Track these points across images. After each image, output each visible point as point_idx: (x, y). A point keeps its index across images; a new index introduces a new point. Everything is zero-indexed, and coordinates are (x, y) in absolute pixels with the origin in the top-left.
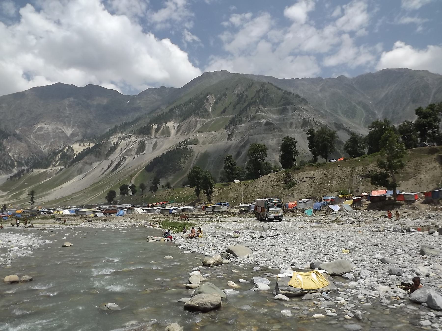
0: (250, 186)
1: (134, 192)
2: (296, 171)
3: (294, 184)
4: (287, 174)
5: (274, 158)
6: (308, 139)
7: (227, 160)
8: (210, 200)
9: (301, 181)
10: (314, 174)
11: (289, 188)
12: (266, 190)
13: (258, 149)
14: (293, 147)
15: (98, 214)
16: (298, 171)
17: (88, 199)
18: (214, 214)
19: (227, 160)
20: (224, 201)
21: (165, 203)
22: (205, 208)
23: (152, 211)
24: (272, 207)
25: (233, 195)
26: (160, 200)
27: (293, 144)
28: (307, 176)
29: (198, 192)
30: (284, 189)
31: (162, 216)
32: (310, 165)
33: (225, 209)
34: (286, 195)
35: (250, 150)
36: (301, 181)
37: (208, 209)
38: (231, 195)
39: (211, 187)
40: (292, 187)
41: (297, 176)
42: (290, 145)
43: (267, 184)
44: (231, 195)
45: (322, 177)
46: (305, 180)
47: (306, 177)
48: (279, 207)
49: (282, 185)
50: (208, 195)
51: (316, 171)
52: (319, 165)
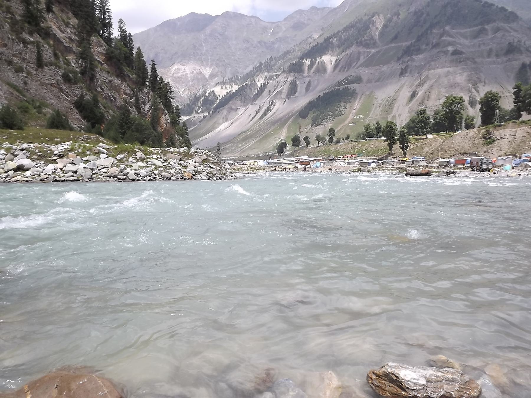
1: (308, 144)
2: (497, 128)
3: (494, 141)
4: (487, 131)
5: (474, 112)
6: (514, 93)
8: (405, 154)
9: (501, 138)
10: (516, 132)
11: (488, 145)
12: (464, 146)
13: (454, 101)
14: (496, 102)
16: (500, 128)
18: (414, 167)
19: (421, 114)
21: (354, 156)
22: (403, 162)
23: (352, 164)
24: (485, 163)
26: (345, 153)
27: (496, 99)
28: (509, 134)
29: (390, 146)
30: (483, 145)
32: (513, 122)
34: (485, 152)
35: (444, 103)
36: (501, 138)
37: (406, 163)
38: (426, 150)
39: (407, 142)
40: (491, 144)
41: (497, 133)
42: (493, 100)
43: (465, 141)
44: (426, 150)
45: (524, 134)
47: (507, 135)
48: (490, 163)
49: (482, 142)
50: (403, 150)
51: (519, 129)
52: (523, 122)
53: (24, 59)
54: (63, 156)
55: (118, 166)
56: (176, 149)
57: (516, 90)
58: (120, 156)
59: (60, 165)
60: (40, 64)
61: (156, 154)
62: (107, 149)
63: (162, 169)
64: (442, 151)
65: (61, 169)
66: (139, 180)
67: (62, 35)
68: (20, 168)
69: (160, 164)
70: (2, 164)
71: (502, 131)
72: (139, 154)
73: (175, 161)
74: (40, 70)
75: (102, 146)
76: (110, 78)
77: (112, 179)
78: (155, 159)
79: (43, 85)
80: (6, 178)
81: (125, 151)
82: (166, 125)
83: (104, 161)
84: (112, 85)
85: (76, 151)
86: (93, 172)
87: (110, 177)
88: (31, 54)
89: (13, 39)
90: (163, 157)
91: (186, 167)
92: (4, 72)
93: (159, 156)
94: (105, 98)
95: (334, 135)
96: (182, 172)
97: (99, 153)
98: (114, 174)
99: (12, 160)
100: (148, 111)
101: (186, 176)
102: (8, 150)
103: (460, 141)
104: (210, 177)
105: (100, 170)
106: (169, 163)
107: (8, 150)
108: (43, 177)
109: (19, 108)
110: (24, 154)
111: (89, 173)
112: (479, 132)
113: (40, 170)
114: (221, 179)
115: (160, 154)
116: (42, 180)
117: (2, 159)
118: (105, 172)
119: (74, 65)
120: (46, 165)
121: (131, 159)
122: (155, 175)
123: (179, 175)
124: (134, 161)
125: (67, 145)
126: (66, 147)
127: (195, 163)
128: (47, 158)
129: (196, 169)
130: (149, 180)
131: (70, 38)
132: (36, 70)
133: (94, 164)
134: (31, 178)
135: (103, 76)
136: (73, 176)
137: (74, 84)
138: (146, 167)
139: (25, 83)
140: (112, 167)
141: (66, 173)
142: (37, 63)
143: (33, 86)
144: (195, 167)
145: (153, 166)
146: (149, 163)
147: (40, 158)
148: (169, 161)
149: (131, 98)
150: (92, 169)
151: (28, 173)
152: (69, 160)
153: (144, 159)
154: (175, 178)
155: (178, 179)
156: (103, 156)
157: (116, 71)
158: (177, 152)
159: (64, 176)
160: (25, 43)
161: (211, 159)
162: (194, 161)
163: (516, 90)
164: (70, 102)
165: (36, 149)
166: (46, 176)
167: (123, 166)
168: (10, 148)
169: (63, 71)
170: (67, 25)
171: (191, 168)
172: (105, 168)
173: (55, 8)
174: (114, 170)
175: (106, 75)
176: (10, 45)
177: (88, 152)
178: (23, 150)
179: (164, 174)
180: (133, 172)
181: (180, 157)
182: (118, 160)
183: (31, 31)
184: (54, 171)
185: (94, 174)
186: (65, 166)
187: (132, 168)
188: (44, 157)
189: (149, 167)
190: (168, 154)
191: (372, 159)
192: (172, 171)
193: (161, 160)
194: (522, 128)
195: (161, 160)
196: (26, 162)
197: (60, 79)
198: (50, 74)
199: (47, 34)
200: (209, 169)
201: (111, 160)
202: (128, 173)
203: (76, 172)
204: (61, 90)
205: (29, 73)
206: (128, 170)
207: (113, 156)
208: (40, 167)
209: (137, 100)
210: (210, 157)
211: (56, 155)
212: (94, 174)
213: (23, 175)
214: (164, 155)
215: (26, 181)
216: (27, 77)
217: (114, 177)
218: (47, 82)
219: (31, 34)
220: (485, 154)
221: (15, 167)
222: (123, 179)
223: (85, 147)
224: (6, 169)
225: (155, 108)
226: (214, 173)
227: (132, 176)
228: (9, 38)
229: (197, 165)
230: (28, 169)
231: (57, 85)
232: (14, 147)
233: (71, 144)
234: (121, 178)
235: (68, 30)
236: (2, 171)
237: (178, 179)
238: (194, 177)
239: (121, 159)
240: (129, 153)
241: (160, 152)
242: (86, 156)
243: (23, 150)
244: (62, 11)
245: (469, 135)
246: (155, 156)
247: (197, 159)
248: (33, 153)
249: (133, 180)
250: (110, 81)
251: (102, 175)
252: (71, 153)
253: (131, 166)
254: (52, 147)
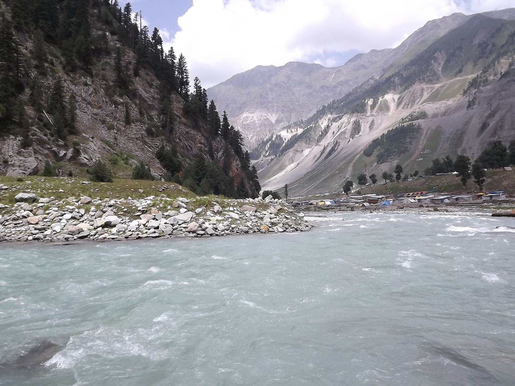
1: (374, 181)
7: (496, 146)
15: (365, 204)
17: (306, 189)
19: (496, 146)
20: (498, 190)
21: (424, 192)
23: (423, 201)
25: (507, 183)
26: (414, 189)
29: (464, 180)
31: (433, 205)
33: (503, 197)
37: (484, 198)
38: (505, 183)
39: (483, 176)
50: (479, 185)
53: (115, 118)
54: (146, 212)
55: (196, 220)
56: (251, 200)
58: (199, 210)
59: (143, 221)
60: (128, 121)
61: (233, 206)
62: (186, 203)
63: (239, 222)
65: (144, 225)
66: (217, 235)
67: (147, 95)
68: (108, 225)
69: (237, 217)
70: (92, 221)
72: (217, 208)
73: (251, 213)
74: (128, 126)
75: (181, 200)
76: (187, 130)
77: (191, 235)
78: (232, 211)
79: (130, 139)
80: (95, 235)
81: (203, 204)
82: (237, 170)
83: (184, 215)
84: (188, 136)
85: (158, 207)
86: (174, 228)
87: (189, 232)
88: (121, 114)
89: (106, 102)
90: (239, 209)
91: (262, 219)
92: (99, 129)
93: (235, 208)
94: (183, 147)
95: (401, 172)
96: (259, 224)
97: (179, 207)
98: (193, 230)
99: (101, 216)
100: (221, 158)
101: (263, 228)
102: (98, 206)
104: (287, 229)
105: (179, 225)
106: (245, 215)
107: (98, 206)
108: (128, 233)
109: (109, 161)
110: (112, 210)
111: (170, 228)
113: (126, 226)
114: (297, 230)
115: (236, 206)
116: (126, 238)
117: (92, 216)
118: (184, 228)
119: (155, 120)
120: (131, 221)
121: (209, 213)
122: (233, 229)
123: (255, 228)
124: (212, 215)
125: (149, 200)
126: (149, 202)
127: (271, 213)
128: (132, 213)
129: (272, 221)
130: (227, 234)
131: (153, 97)
132: (125, 127)
133: (175, 220)
134: (118, 235)
135: (181, 128)
136: (155, 232)
137: (156, 137)
138: (223, 220)
139: (116, 139)
140: (191, 221)
141: (149, 229)
142: (126, 121)
143: (122, 140)
144: (271, 219)
145: (230, 220)
146: (227, 216)
147: (126, 213)
148: (245, 212)
149: (205, 147)
150: (173, 225)
151: (114, 230)
152: (152, 216)
153: (222, 212)
154: (252, 232)
155: (255, 232)
156: (182, 210)
157: (192, 123)
158: (253, 203)
159: (146, 233)
160: (116, 104)
161: (286, 208)
162: (270, 211)
164: (153, 153)
165: (122, 205)
166: (131, 233)
167: (201, 220)
168: (100, 205)
169: (147, 126)
170: (151, 86)
171: (267, 220)
172: (185, 222)
173: (142, 73)
174: (193, 225)
175: (183, 127)
176: (104, 107)
177: (169, 207)
178: (110, 206)
179: (241, 227)
180: (211, 226)
181: (255, 208)
182: (197, 214)
183: (121, 94)
184: (137, 227)
185: (174, 229)
186: (148, 222)
187: (211, 222)
188: (129, 213)
189: (226, 220)
190: (244, 206)
191: (445, 195)
192: (249, 224)
193: (238, 212)
195: (238, 212)
196: (113, 219)
197: (144, 132)
198: (137, 130)
199: (134, 95)
200: (285, 220)
201: (191, 214)
202: (206, 228)
203: (157, 228)
204: (145, 143)
205: (119, 130)
206: (207, 224)
207: (192, 210)
208: (125, 223)
209: (211, 147)
210: (285, 206)
211: (140, 210)
212: (174, 229)
213: (110, 231)
214: (240, 207)
215: (113, 239)
216: (117, 133)
217: (194, 232)
218: (133, 136)
219: (121, 96)
221: (103, 223)
222: (202, 235)
223: (166, 202)
224: (95, 225)
225: (227, 154)
226: (290, 224)
227: (210, 231)
228: (103, 101)
229: (273, 216)
230: (115, 226)
231: (142, 139)
232: (103, 204)
233: (153, 198)
234: (200, 234)
235: (152, 91)
236: (92, 227)
237: (255, 232)
238: (271, 229)
239: (200, 213)
240: (207, 206)
241: (236, 204)
242: (167, 211)
243: (110, 206)
244: (147, 74)
246: (231, 209)
247: (272, 210)
248: (119, 209)
249: (211, 235)
250: (187, 132)
251: (182, 230)
252: (153, 208)
253: (210, 220)
254: (137, 203)
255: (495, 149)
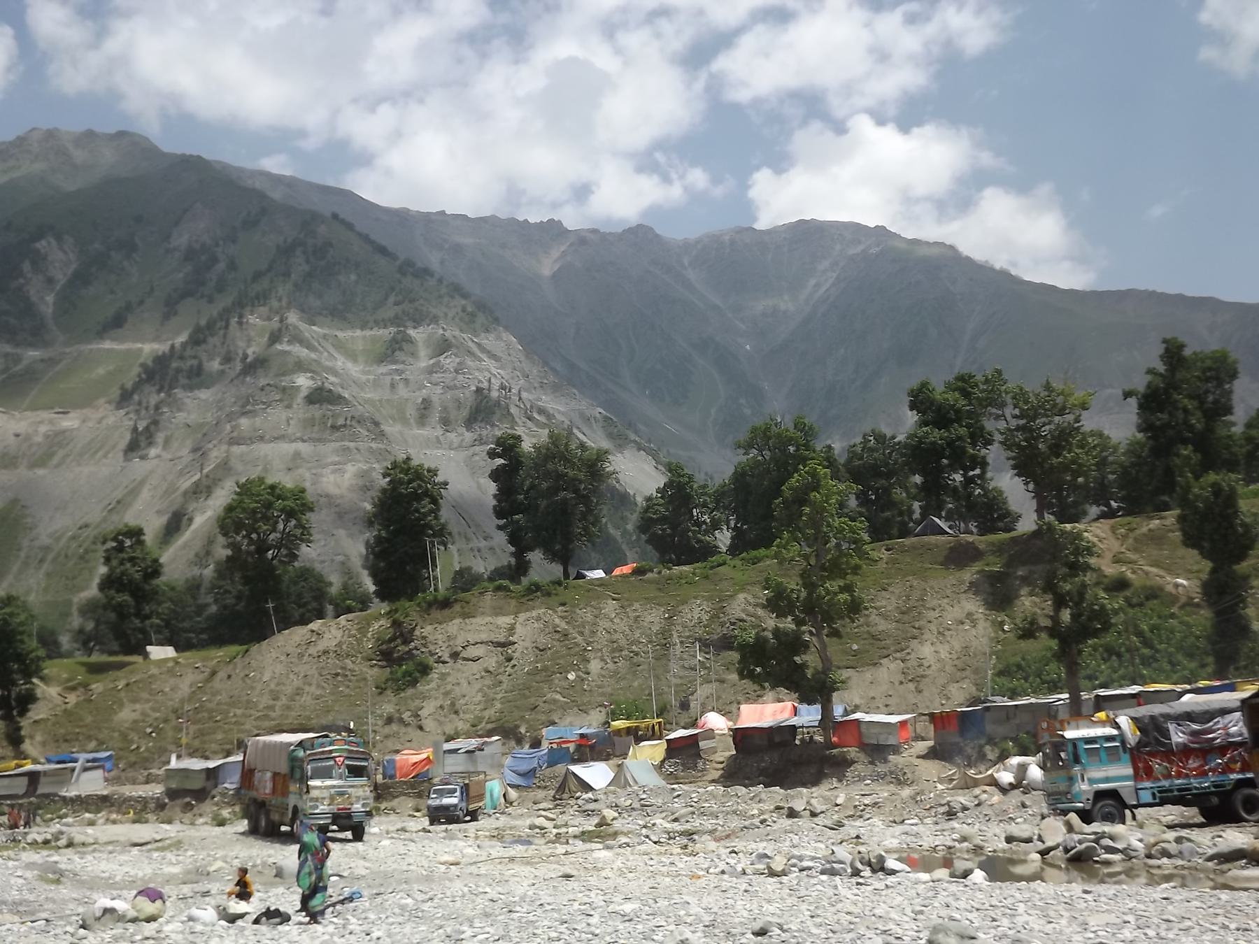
0: (222, 674)
2: (436, 614)
3: (425, 670)
4: (396, 624)
6: (495, 475)
7: (120, 548)
9: (455, 656)
10: (512, 629)
11: (399, 690)
12: (299, 692)
13: (269, 506)
14: (426, 505)
16: (447, 612)
19: (120, 548)
20: (93, 744)
24: (325, 774)
27: (426, 493)
28: (484, 637)
30: (381, 690)
32: (499, 588)
33: (91, 783)
34: (389, 720)
35: (230, 509)
38: (126, 714)
39: (28, 674)
40: (414, 683)
41: (437, 634)
42: (417, 497)
43: (302, 669)
44: (126, 714)
45: (543, 641)
46: (472, 652)
47: (477, 642)
48: (356, 772)
49: (374, 673)
51: (522, 617)
52: (535, 588)
57: (500, 461)
64: (203, 723)
71: (454, 626)
103: (279, 669)
112: (363, 630)
163: (500, 461)
194: (534, 613)
220: (387, 730)
245: (322, 646)
255: (114, 563)
